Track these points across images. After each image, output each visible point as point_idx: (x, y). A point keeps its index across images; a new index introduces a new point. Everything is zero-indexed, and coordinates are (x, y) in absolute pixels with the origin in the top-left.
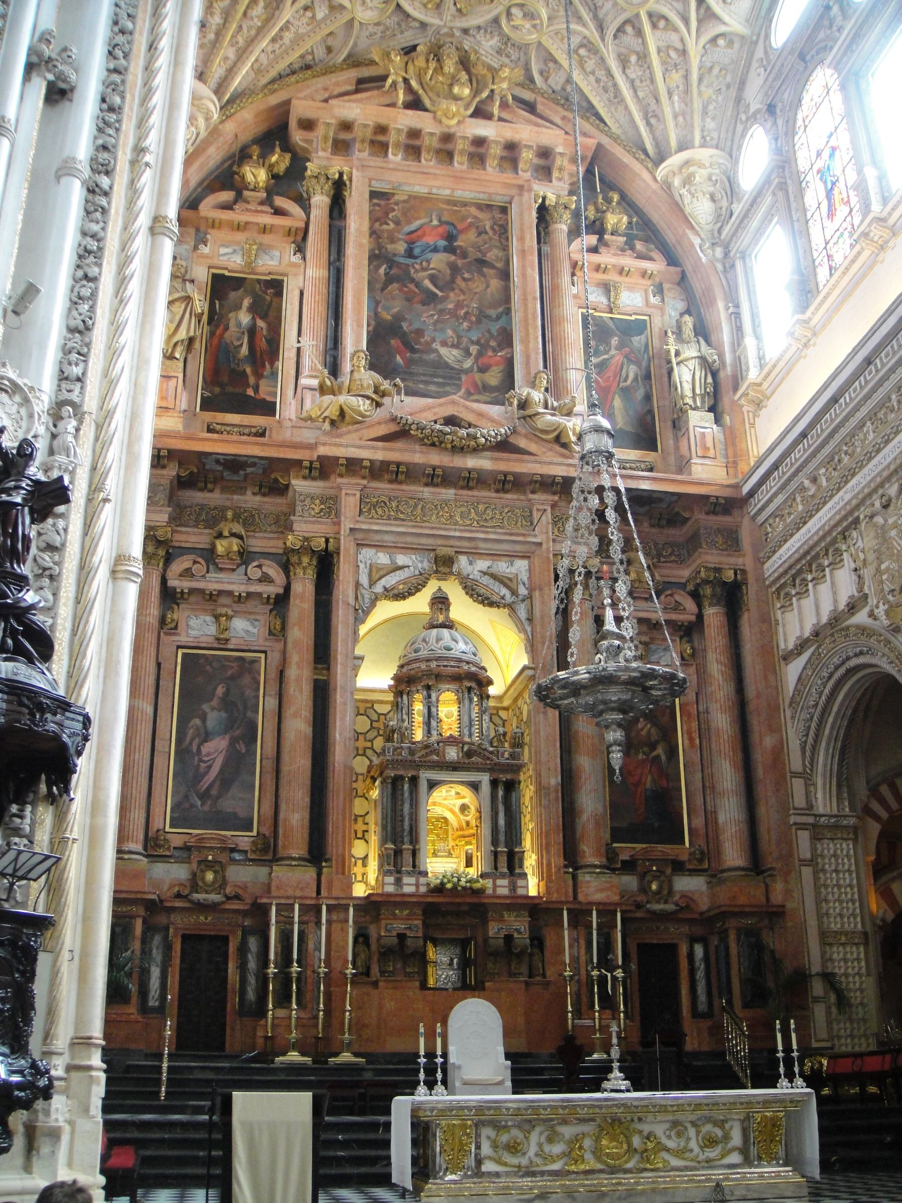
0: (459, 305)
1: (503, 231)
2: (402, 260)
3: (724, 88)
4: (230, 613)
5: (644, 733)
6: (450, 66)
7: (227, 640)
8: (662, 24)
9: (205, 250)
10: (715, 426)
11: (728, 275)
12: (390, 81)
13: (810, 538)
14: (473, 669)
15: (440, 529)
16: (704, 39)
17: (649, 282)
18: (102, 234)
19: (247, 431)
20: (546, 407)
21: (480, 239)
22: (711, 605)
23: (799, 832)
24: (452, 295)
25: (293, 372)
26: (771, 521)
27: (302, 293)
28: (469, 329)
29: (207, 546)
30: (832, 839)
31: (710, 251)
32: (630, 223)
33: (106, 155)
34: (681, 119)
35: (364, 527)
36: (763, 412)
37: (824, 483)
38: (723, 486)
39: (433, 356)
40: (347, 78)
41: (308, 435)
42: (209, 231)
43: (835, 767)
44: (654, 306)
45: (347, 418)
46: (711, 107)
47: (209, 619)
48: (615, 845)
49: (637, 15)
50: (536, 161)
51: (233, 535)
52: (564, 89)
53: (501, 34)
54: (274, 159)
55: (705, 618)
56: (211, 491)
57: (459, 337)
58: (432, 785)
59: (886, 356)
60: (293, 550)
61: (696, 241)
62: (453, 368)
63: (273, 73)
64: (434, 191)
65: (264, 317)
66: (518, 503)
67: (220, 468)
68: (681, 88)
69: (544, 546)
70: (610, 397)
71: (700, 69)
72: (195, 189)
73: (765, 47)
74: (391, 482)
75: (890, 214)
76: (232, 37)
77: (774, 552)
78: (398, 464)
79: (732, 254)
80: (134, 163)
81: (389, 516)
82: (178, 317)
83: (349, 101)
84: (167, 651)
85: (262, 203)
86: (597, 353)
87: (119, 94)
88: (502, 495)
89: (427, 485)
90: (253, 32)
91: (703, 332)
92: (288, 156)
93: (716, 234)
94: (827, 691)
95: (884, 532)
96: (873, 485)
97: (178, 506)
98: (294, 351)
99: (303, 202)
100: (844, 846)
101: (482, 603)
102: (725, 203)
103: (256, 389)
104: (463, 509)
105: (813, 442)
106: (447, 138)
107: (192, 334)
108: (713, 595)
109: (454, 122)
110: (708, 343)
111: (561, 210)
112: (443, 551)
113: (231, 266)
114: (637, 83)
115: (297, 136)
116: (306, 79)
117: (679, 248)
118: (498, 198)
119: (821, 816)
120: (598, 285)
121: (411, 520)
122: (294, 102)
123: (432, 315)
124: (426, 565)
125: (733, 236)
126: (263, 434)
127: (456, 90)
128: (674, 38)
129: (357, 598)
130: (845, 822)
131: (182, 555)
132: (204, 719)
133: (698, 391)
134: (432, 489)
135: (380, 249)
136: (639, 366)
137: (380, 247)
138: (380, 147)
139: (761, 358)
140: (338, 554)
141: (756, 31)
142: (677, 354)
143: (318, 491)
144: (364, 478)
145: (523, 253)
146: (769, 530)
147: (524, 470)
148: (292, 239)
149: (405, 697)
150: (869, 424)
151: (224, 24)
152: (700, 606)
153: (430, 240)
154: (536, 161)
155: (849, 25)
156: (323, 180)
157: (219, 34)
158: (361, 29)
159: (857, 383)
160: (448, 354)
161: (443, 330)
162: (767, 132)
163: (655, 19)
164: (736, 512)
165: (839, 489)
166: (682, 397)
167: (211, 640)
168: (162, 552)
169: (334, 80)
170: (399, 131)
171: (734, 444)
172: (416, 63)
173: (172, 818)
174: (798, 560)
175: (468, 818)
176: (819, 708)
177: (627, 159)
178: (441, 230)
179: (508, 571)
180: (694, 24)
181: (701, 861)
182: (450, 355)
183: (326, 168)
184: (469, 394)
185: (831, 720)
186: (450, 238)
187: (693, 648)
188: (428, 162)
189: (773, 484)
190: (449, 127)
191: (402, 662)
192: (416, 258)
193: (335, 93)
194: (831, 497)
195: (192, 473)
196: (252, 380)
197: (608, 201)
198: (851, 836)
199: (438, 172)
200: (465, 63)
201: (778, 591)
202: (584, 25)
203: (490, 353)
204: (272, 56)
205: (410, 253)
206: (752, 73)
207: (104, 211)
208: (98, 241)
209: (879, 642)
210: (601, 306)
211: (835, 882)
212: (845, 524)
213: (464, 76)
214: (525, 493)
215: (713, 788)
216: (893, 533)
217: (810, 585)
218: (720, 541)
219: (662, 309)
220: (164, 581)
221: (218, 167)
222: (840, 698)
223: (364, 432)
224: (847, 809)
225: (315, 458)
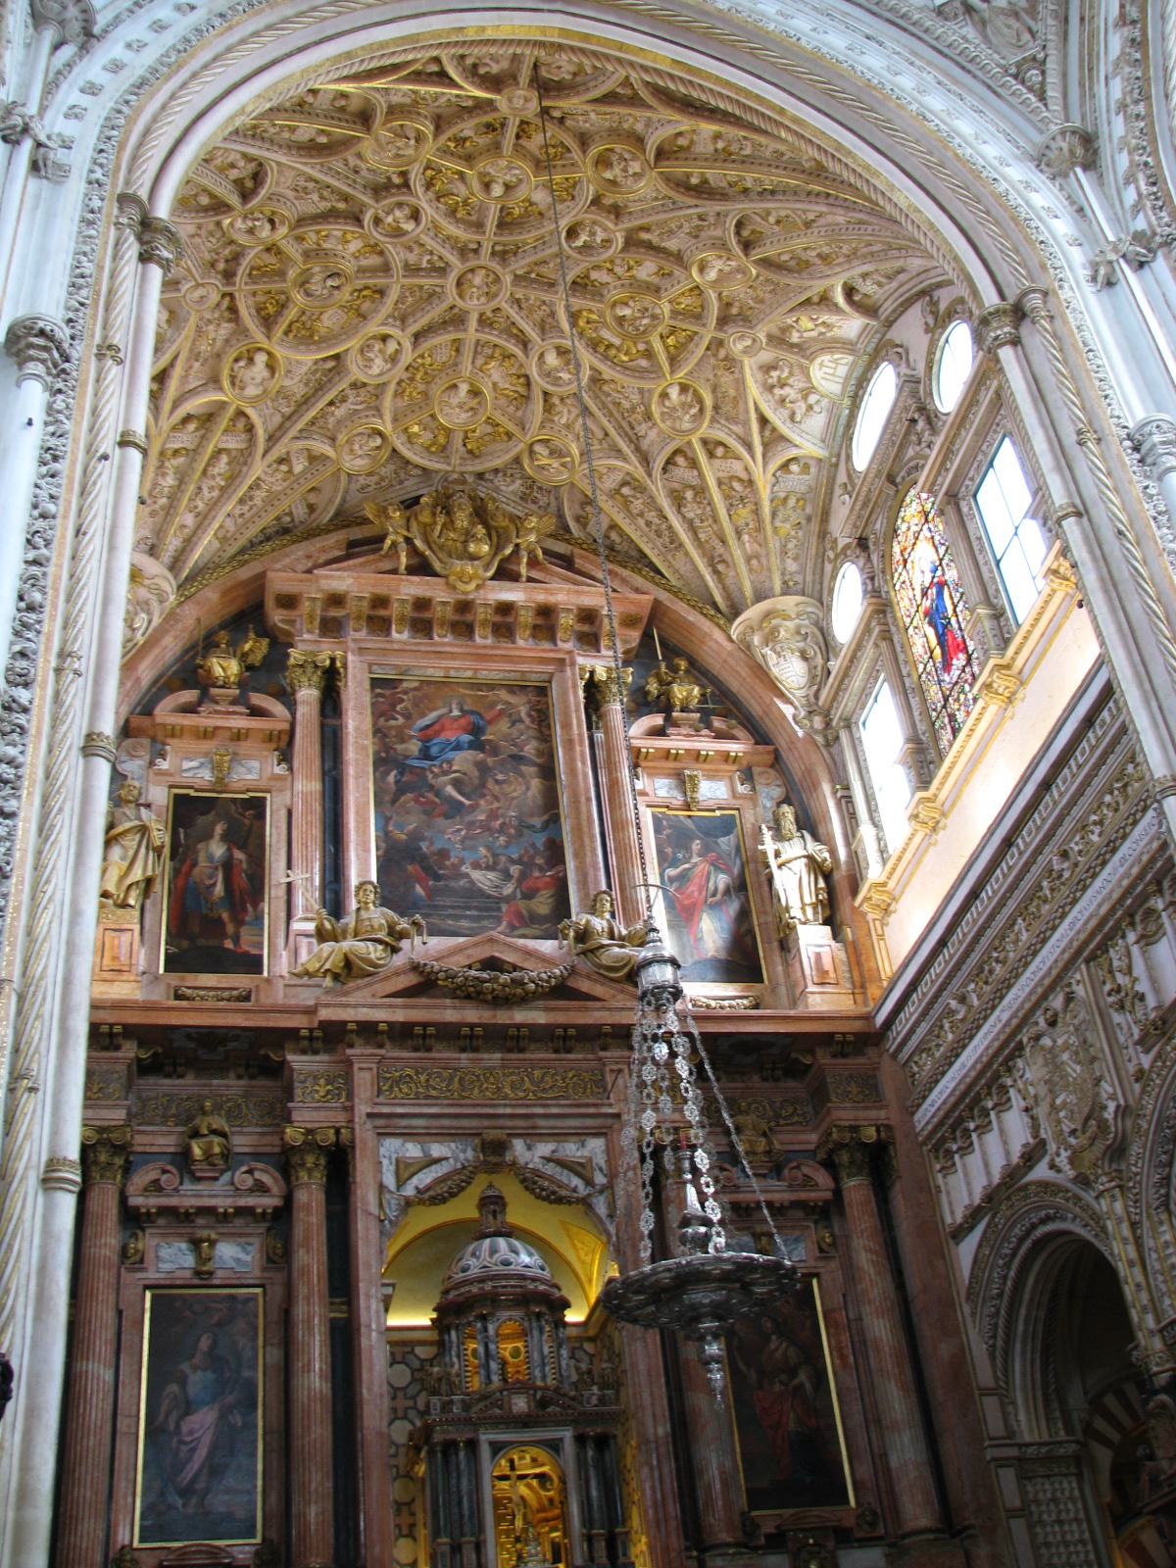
0: (493, 815)
1: (542, 718)
2: (416, 763)
3: (804, 522)
4: (213, 1236)
5: (778, 1355)
6: (462, 519)
7: (211, 1273)
8: (720, 451)
9: (164, 765)
10: (833, 943)
11: (832, 750)
12: (388, 542)
13: (966, 1076)
14: (542, 1287)
15: (486, 1106)
16: (773, 466)
17: (735, 768)
18: (21, 759)
19: (226, 994)
20: (612, 937)
21: (514, 732)
22: (849, 1176)
23: (1001, 1471)
24: (482, 802)
25: (283, 915)
26: (916, 1059)
27: (290, 813)
28: (508, 844)
29: (179, 1150)
30: (1048, 1477)
31: (806, 722)
32: (703, 695)
33: (24, 663)
34: (754, 562)
35: (386, 1110)
36: (892, 919)
37: (976, 1002)
38: (848, 1018)
39: (462, 883)
40: (334, 541)
41: (307, 997)
42: (169, 741)
43: (1038, 1376)
44: (743, 797)
45: (355, 969)
46: (790, 546)
47: (184, 1246)
48: (754, 1513)
49: (689, 443)
50: (579, 627)
51: (214, 1132)
52: (607, 537)
53: (526, 477)
54: (247, 647)
55: (845, 1193)
56: (181, 1076)
57: (495, 855)
58: (497, 1448)
59: (1029, 834)
60: (293, 1147)
61: (788, 711)
62: (489, 896)
63: (242, 541)
64: (452, 673)
66: (585, 1065)
67: (193, 1046)
70: (696, 919)
71: (772, 501)
72: (149, 690)
73: (848, 470)
74: (416, 1049)
75: (1013, 659)
76: (190, 500)
77: (925, 1098)
78: (425, 1025)
79: (834, 723)
80: (58, 671)
81: (417, 1093)
82: (131, 853)
83: (339, 570)
84: (129, 1294)
85: (234, 702)
86: (674, 863)
87: (39, 590)
88: (563, 1056)
89: (463, 1050)
90: (216, 493)
91: (809, 824)
92: (265, 642)
93: (812, 700)
94: (1012, 1274)
95: (1055, 1057)
96: (1034, 998)
97: (139, 1098)
98: (284, 888)
99: (287, 697)
100: (1065, 1485)
101: (545, 1199)
102: (819, 661)
103: (236, 939)
104: (514, 1078)
105: (954, 950)
106: (464, 606)
107: (149, 873)
108: (852, 1163)
109: (472, 586)
110: (816, 838)
111: (614, 688)
112: (492, 1135)
113: (198, 783)
114: (697, 523)
115: (277, 617)
116: (285, 546)
117: (767, 720)
118: (533, 677)
119: (1031, 1444)
120: (668, 776)
121: (446, 1098)
122: (270, 574)
123: (459, 830)
124: (470, 1154)
125: (834, 699)
126: (247, 998)
127: (472, 547)
129: (381, 1205)
130: (1062, 1451)
131: (146, 1163)
132: (183, 1382)
133: (807, 900)
134: (471, 1055)
135: (387, 752)
136: (727, 871)
137: (387, 748)
138: (379, 624)
139: (883, 851)
140: (353, 1148)
141: (835, 450)
142: (777, 854)
143: (322, 1068)
144: (381, 1046)
146: (916, 1069)
147: (590, 1021)
148: (274, 745)
149: (453, 1333)
150: (1020, 921)
151: (179, 486)
152: (836, 1179)
153: (450, 735)
154: (579, 627)
155: (939, 441)
156: (310, 670)
157: (173, 498)
158: (349, 482)
159: (998, 871)
160: (482, 879)
161: (473, 849)
162: (862, 570)
163: (711, 446)
164: (871, 1052)
165: (994, 1008)
166: (787, 909)
167: (188, 1274)
168: (119, 1161)
169: (318, 545)
171: (859, 964)
172: (421, 518)
173: (142, 1528)
174: (955, 1106)
175: (551, 1493)
176: (1006, 1297)
177: (693, 616)
178: (463, 721)
179: (579, 1154)
180: (758, 449)
181: (873, 1524)
182: (483, 879)
183: (314, 654)
184: (512, 927)
185: (1023, 1311)
186: (476, 731)
187: (832, 1235)
188: (443, 639)
189: (912, 1010)
190: (466, 593)
191: (448, 1285)
192: (436, 758)
193: (321, 561)
194: (986, 1018)
195: (155, 1054)
196: (230, 929)
197: (674, 669)
198: (1073, 1469)
199: (456, 650)
200: (481, 514)
201: (936, 1148)
202: (625, 459)
203: (537, 874)
204: (240, 520)
205: (425, 754)
206: (836, 503)
207: (23, 730)
208: (16, 767)
209: (1067, 1200)
210: (675, 802)
211: (1059, 1537)
212: (1007, 1052)
213: (480, 530)
214: (593, 1051)
215: (878, 1421)
216: (1065, 1057)
217: (974, 1136)
218: (855, 1091)
219: (753, 798)
220: (123, 1199)
221: (177, 661)
222: (1031, 1280)
223: (378, 986)
224: (1062, 1433)
225: (316, 1025)
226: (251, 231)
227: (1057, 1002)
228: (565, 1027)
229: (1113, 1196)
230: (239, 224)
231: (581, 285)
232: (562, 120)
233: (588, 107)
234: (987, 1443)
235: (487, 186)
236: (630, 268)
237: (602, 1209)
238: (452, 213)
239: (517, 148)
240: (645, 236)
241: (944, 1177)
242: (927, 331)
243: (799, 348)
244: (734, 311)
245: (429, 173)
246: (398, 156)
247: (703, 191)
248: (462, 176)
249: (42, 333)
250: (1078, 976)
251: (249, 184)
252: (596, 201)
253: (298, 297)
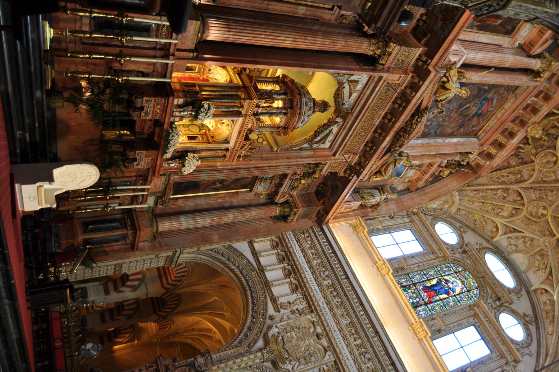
16: (499, 226)
22: (281, 211)
37: (326, 283)
65: (501, 24)
68: (484, 208)
69: (333, 158)
77: (297, 242)
88: (364, 143)
89: (386, 114)
114: (494, 192)
128: (506, 214)
134: (382, 116)
145: (456, 144)
147: (373, 159)
148: (526, 44)
170: (542, 107)
190: (529, 126)
202: (531, 183)
227: (324, 342)
228: (375, 151)
229: (261, 359)
234: (182, 249)
237: (306, 146)
241: (270, 240)
242: (524, 314)
250: (332, 356)
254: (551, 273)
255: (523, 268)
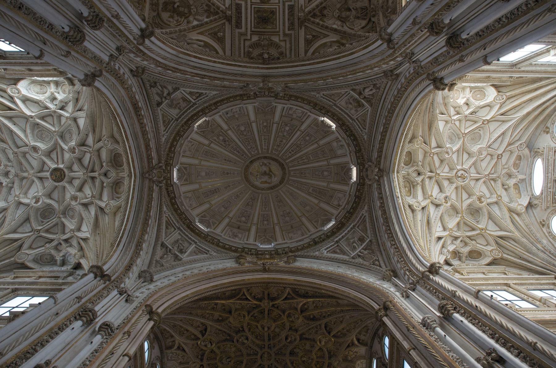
226: (206, 346)
230: (203, 344)
231: (292, 353)
232: (278, 307)
233: (283, 302)
235: (264, 329)
236: (303, 346)
238: (257, 338)
239: (268, 317)
240: (304, 336)
243: (351, 361)
244: (332, 354)
245: (249, 326)
246: (240, 321)
247: (314, 319)
248: (257, 326)
249: (107, 325)
251: (204, 332)
252: (290, 329)
253: (220, 364)
254: (348, 346)
255: (364, 361)
